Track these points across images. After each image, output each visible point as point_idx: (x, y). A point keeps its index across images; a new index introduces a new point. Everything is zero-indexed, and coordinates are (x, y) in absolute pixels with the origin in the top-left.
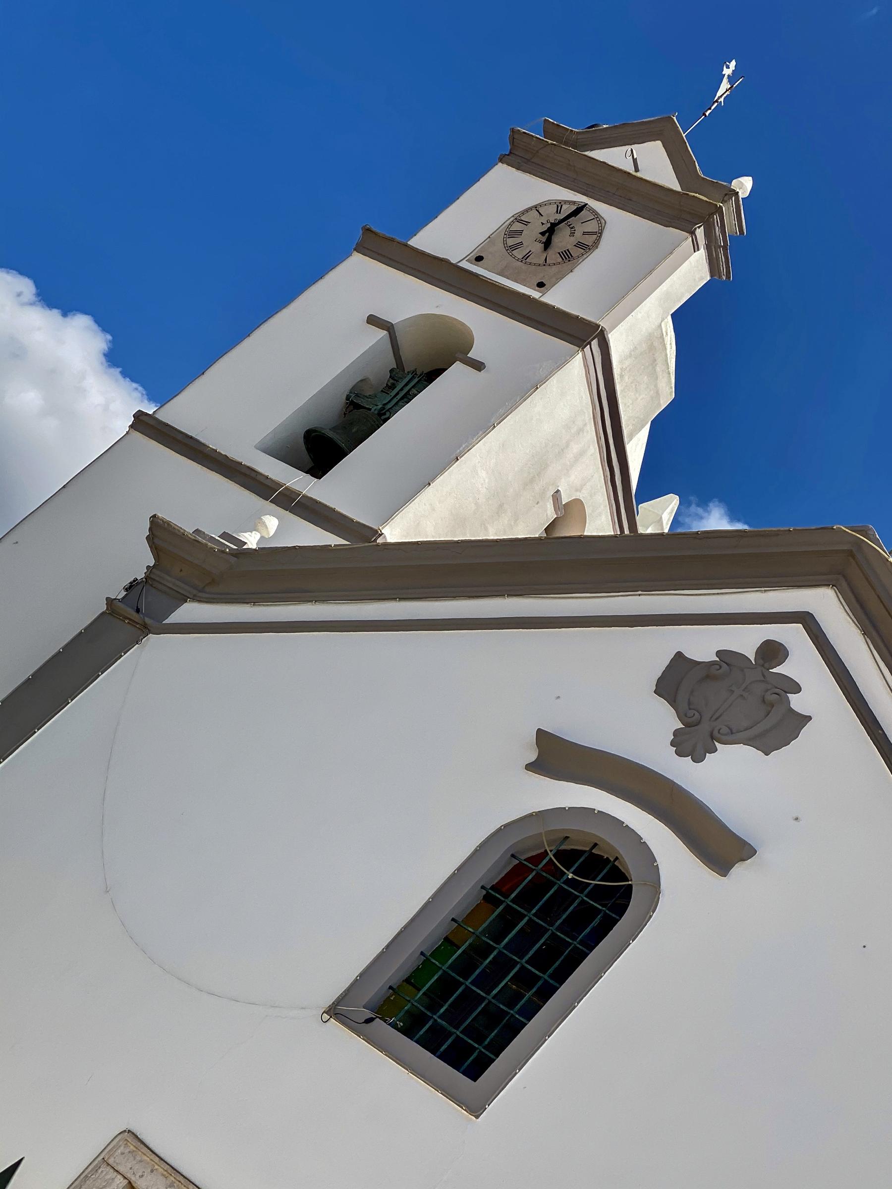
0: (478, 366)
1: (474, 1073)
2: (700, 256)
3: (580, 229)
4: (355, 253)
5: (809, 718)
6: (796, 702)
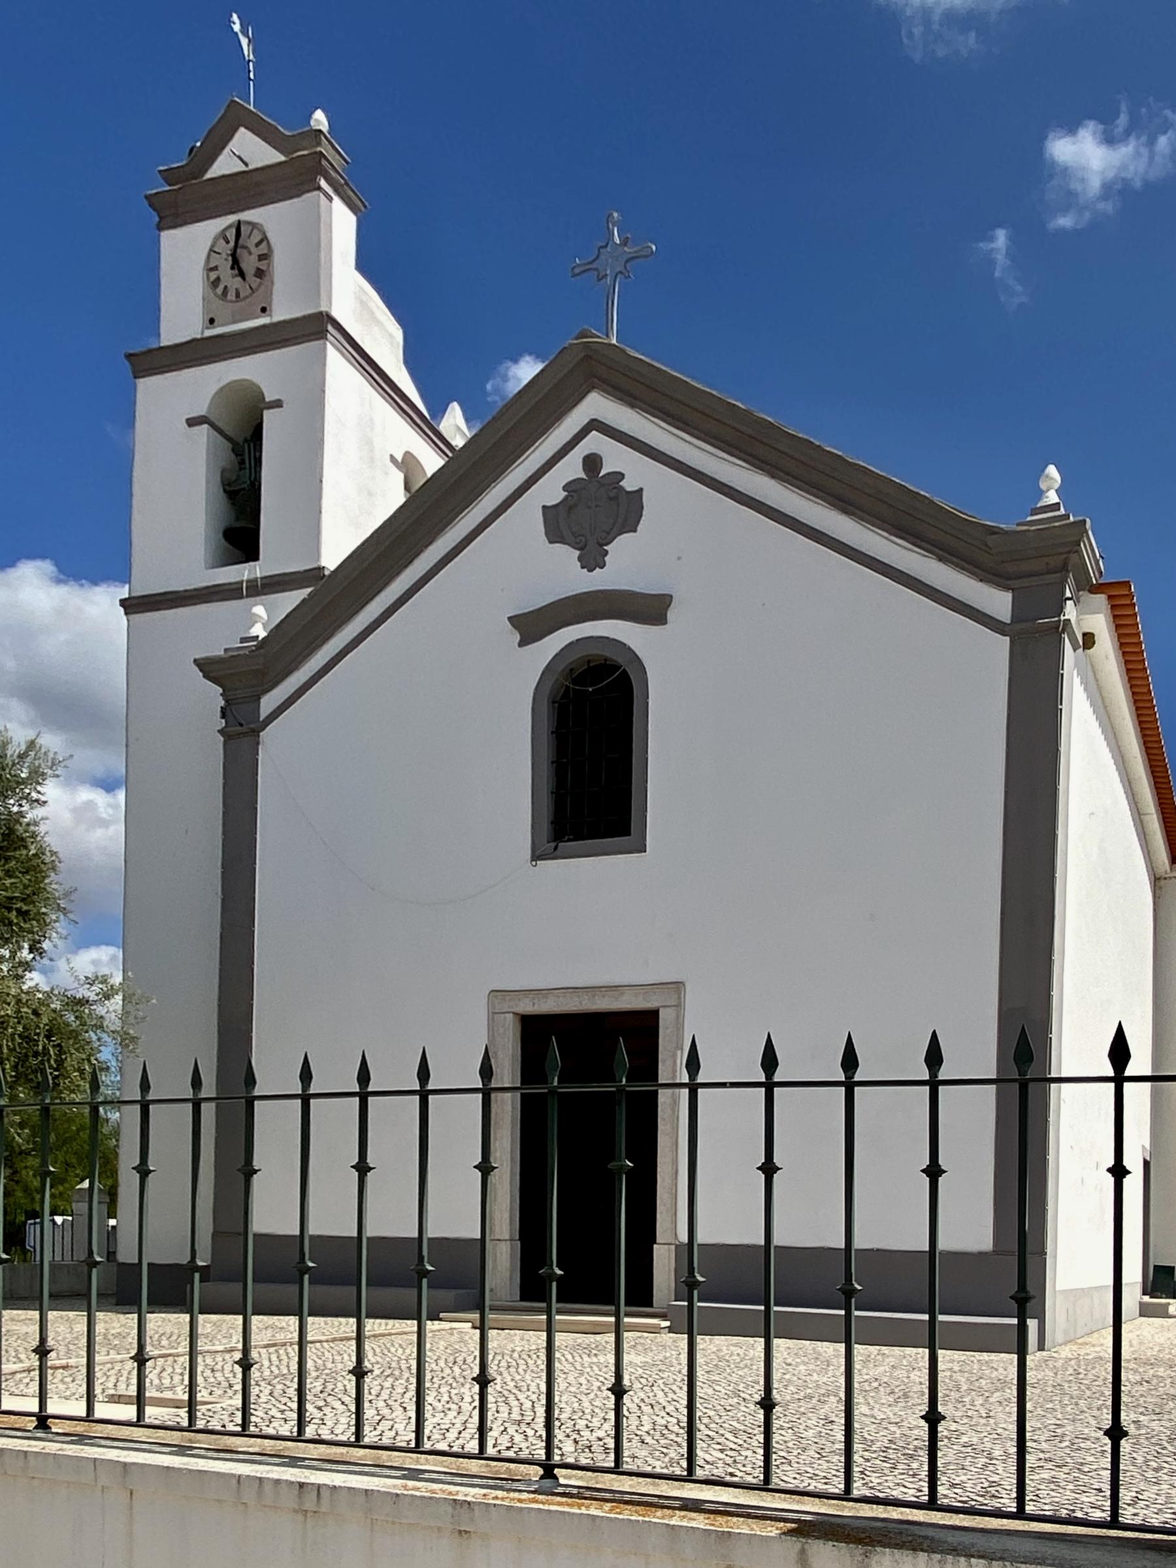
0: (278, 404)
1: (627, 832)
2: (338, 205)
3: (251, 244)
4: (138, 381)
5: (641, 490)
6: (628, 485)
